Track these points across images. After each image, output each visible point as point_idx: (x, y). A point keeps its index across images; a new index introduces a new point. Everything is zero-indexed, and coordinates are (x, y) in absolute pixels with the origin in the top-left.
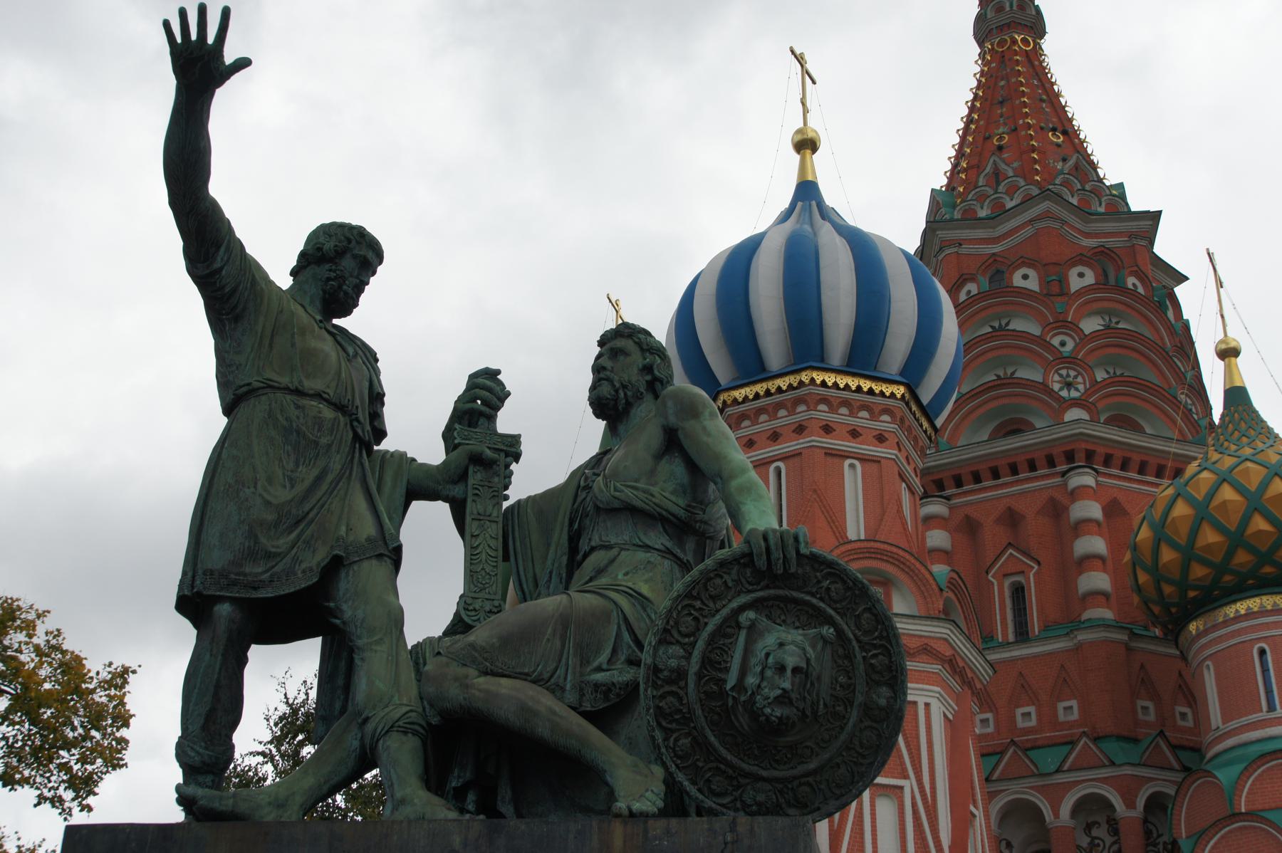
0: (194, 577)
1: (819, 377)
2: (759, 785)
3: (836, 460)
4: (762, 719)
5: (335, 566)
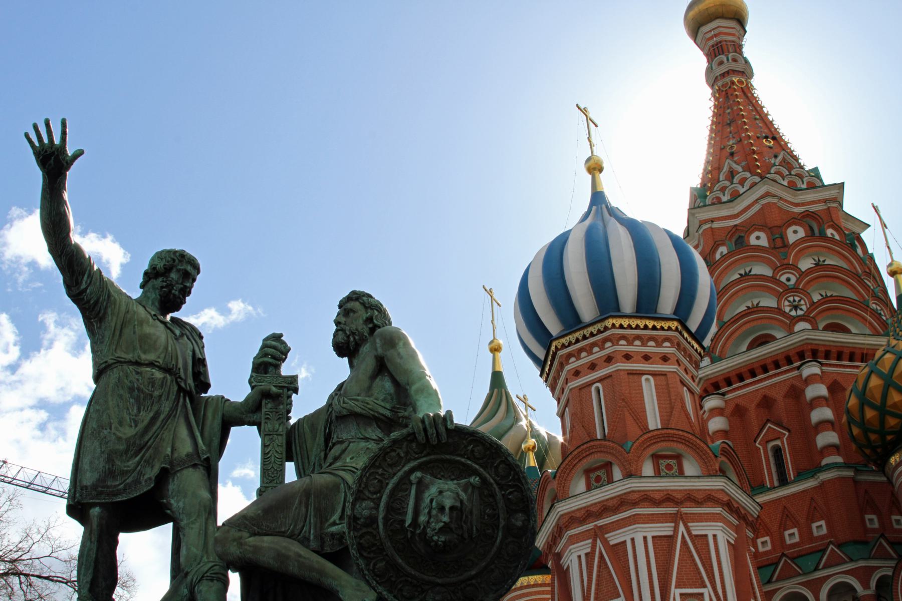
1: (618, 322)
3: (636, 377)
4: (432, 544)
5: (164, 476)
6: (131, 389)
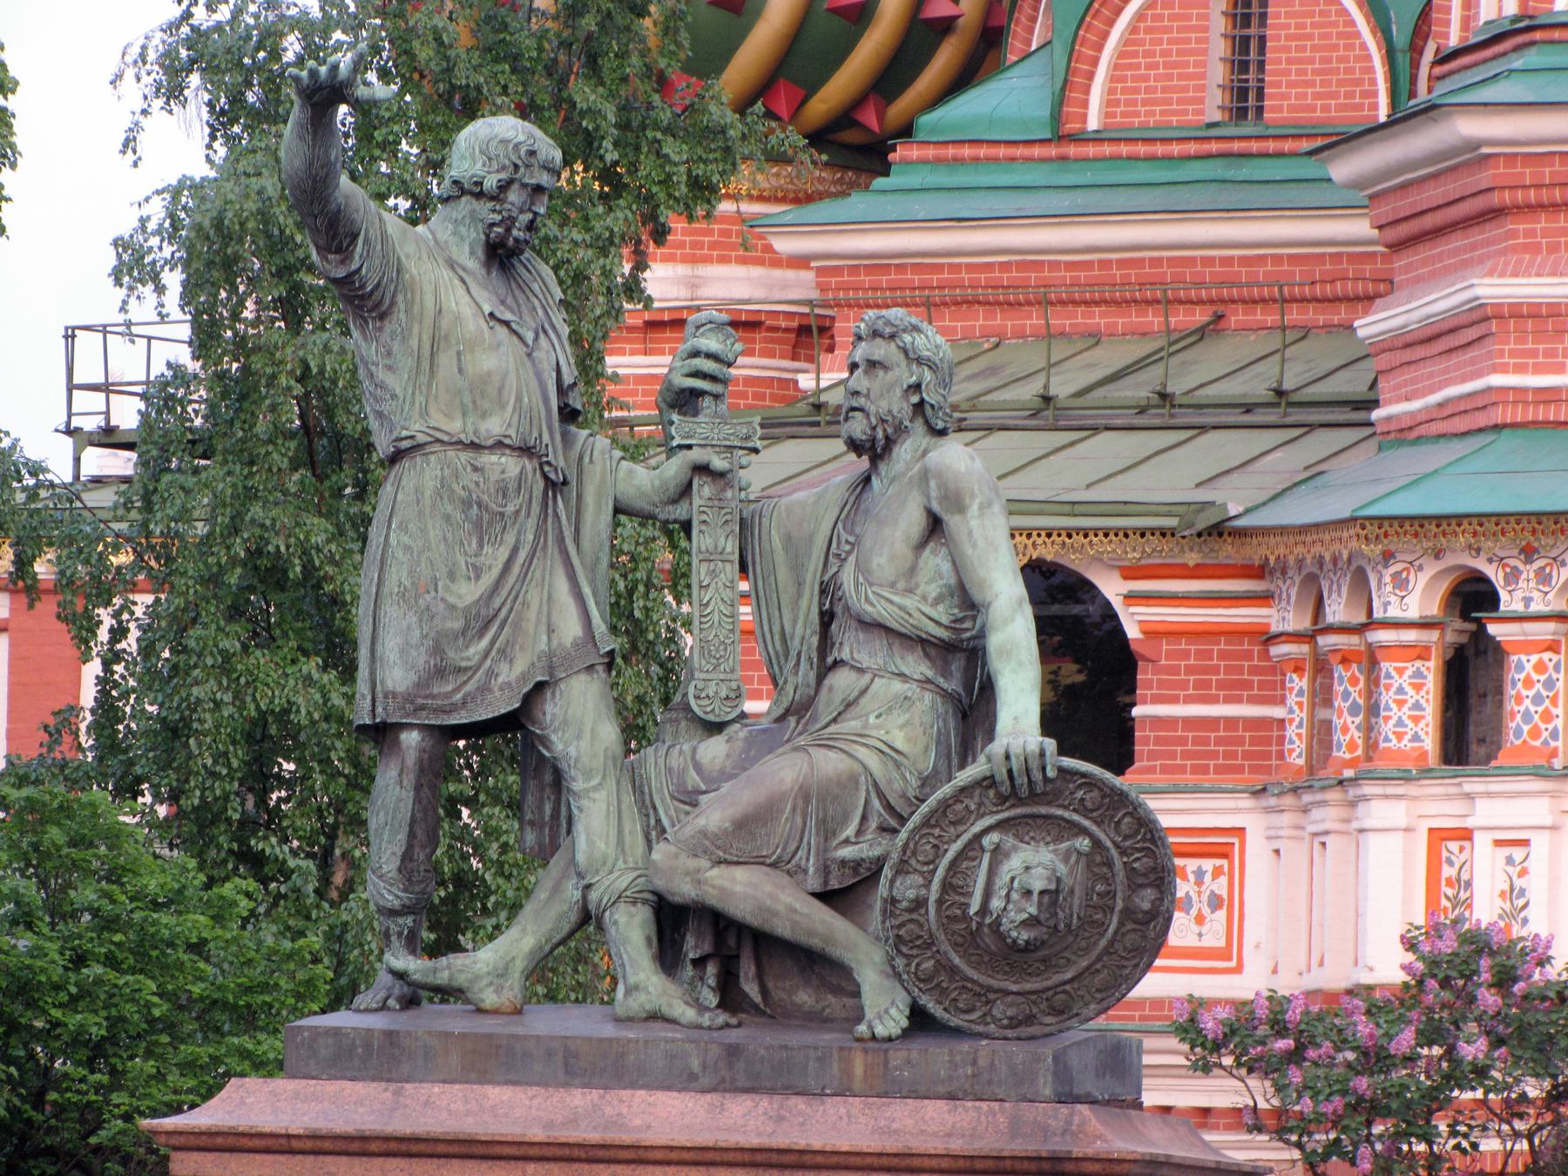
0: (374, 700)
2: (1010, 999)
6: (466, 504)
